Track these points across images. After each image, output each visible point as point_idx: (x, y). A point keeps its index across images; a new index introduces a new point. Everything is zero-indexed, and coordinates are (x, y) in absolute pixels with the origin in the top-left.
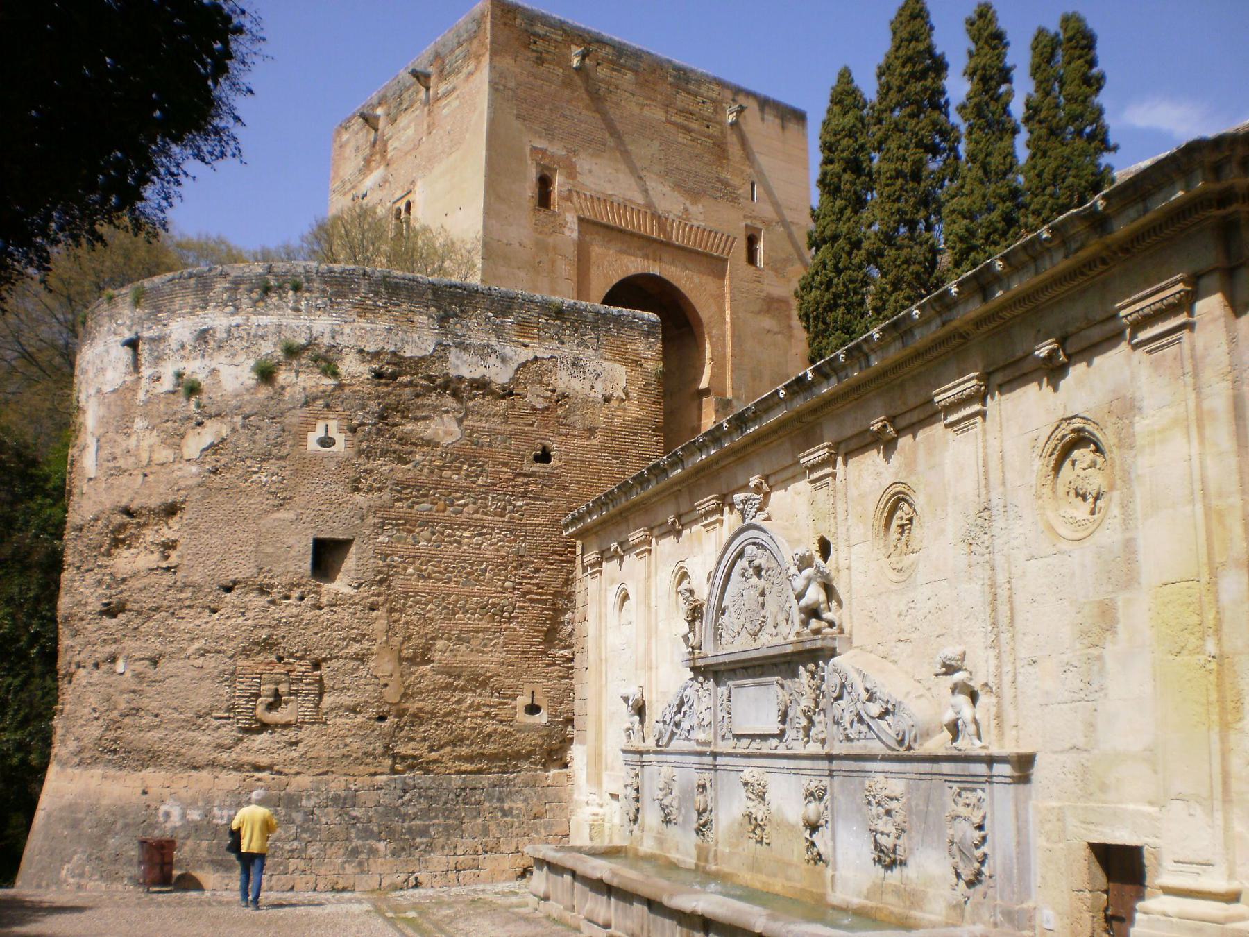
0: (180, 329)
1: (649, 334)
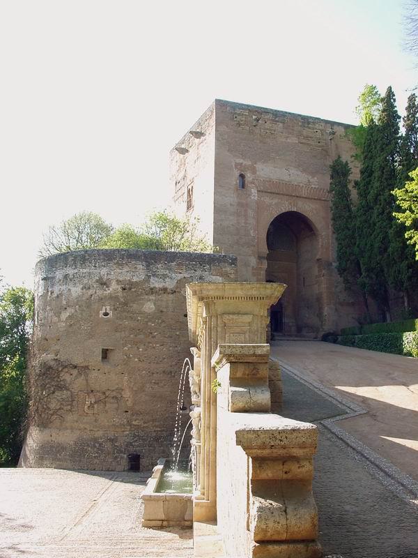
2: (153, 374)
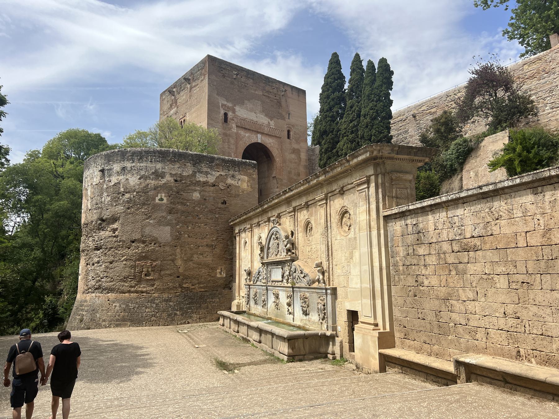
0: (116, 167)
1: (253, 167)
2: (199, 247)
